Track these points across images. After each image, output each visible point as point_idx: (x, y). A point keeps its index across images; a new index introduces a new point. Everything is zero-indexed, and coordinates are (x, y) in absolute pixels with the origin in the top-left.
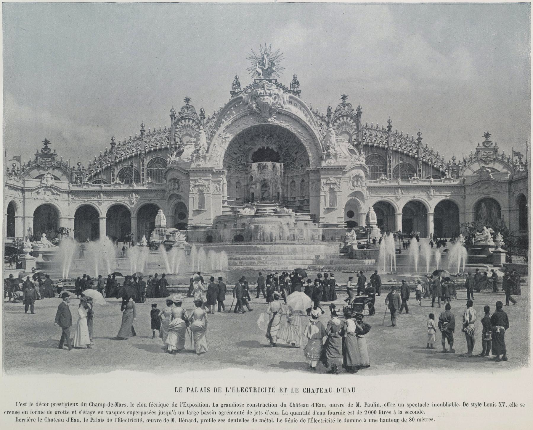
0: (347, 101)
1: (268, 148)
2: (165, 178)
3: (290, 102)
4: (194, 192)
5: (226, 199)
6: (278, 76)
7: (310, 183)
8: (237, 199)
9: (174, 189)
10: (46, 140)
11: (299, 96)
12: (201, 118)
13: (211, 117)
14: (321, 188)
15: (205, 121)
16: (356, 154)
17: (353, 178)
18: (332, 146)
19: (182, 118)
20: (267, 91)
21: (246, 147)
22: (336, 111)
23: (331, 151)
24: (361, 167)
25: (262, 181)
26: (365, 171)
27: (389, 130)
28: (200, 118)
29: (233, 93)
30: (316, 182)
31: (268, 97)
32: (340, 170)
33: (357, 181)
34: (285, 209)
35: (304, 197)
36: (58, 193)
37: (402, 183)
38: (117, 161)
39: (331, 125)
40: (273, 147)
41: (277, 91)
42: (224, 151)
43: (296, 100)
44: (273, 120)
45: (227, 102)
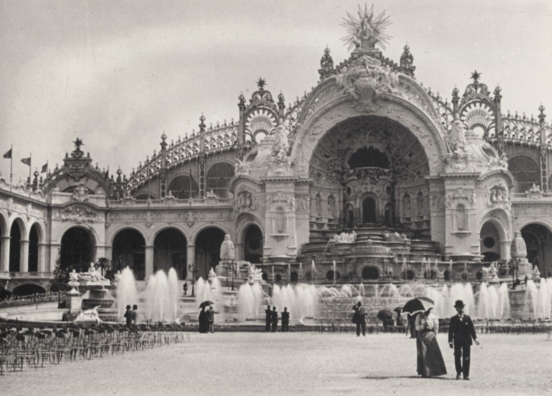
0: (480, 81)
1: (371, 148)
2: (233, 192)
3: (401, 84)
5: (314, 220)
6: (384, 47)
7: (431, 197)
8: (330, 220)
9: (244, 206)
10: (78, 139)
11: (413, 75)
12: (280, 108)
13: (292, 106)
14: (447, 204)
15: (285, 111)
16: (495, 156)
17: (491, 189)
18: (460, 145)
19: (255, 108)
20: (369, 70)
22: (465, 95)
23: (459, 151)
24: (502, 174)
25: (363, 194)
26: (509, 181)
27: (542, 120)
28: (278, 108)
29: (322, 73)
30: (438, 195)
31: (371, 78)
32: (474, 178)
33: (497, 196)
34: (397, 234)
35: (422, 217)
36: (93, 212)
38: (168, 167)
39: (458, 115)
40: (379, 147)
41: (381, 70)
42: (311, 153)
43: (408, 80)
45: (316, 85)
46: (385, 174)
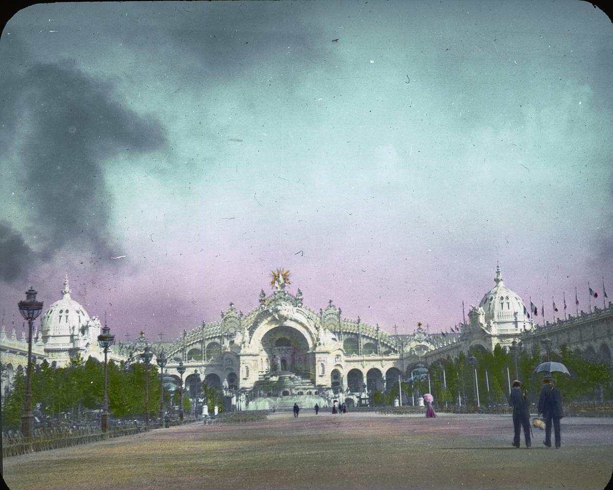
4: (243, 368)
9: (229, 365)
21: (272, 338)
37: (366, 358)
40: (288, 337)
44: (289, 324)
46: (290, 349)
